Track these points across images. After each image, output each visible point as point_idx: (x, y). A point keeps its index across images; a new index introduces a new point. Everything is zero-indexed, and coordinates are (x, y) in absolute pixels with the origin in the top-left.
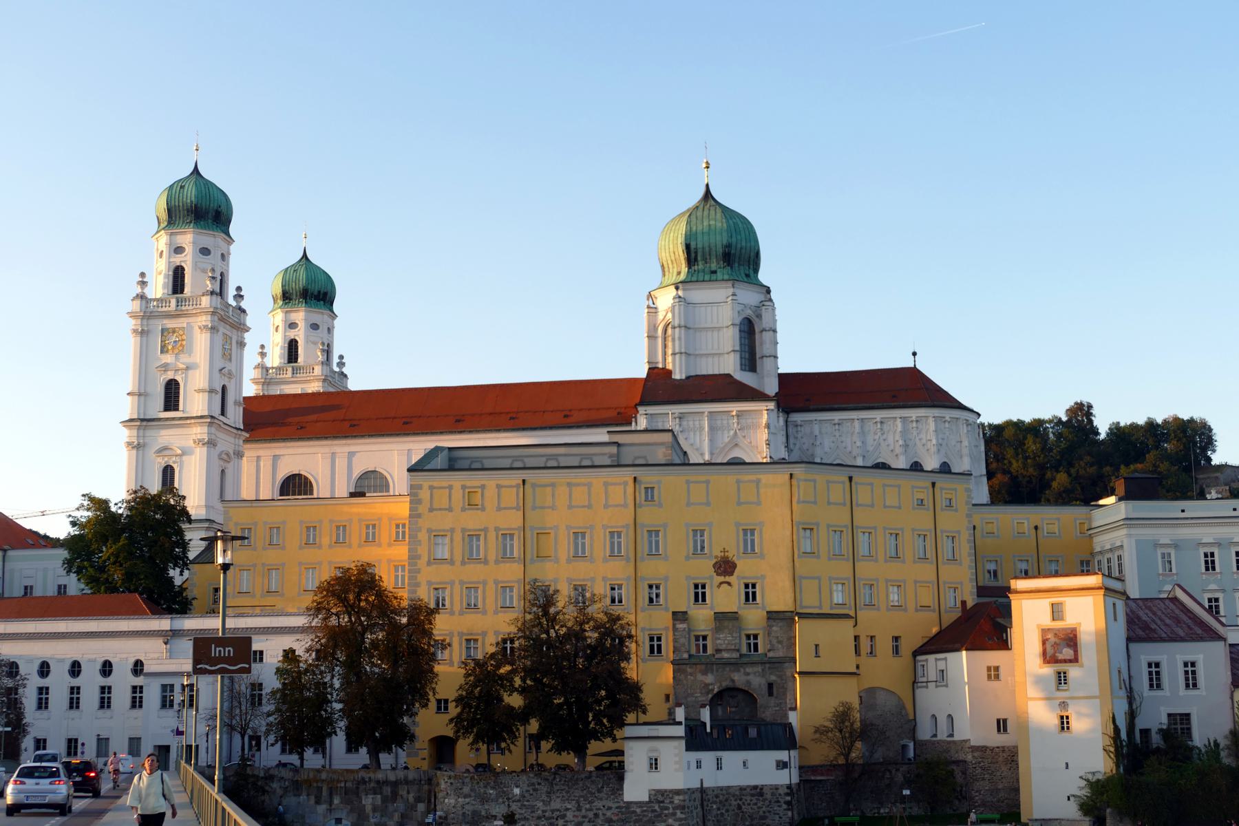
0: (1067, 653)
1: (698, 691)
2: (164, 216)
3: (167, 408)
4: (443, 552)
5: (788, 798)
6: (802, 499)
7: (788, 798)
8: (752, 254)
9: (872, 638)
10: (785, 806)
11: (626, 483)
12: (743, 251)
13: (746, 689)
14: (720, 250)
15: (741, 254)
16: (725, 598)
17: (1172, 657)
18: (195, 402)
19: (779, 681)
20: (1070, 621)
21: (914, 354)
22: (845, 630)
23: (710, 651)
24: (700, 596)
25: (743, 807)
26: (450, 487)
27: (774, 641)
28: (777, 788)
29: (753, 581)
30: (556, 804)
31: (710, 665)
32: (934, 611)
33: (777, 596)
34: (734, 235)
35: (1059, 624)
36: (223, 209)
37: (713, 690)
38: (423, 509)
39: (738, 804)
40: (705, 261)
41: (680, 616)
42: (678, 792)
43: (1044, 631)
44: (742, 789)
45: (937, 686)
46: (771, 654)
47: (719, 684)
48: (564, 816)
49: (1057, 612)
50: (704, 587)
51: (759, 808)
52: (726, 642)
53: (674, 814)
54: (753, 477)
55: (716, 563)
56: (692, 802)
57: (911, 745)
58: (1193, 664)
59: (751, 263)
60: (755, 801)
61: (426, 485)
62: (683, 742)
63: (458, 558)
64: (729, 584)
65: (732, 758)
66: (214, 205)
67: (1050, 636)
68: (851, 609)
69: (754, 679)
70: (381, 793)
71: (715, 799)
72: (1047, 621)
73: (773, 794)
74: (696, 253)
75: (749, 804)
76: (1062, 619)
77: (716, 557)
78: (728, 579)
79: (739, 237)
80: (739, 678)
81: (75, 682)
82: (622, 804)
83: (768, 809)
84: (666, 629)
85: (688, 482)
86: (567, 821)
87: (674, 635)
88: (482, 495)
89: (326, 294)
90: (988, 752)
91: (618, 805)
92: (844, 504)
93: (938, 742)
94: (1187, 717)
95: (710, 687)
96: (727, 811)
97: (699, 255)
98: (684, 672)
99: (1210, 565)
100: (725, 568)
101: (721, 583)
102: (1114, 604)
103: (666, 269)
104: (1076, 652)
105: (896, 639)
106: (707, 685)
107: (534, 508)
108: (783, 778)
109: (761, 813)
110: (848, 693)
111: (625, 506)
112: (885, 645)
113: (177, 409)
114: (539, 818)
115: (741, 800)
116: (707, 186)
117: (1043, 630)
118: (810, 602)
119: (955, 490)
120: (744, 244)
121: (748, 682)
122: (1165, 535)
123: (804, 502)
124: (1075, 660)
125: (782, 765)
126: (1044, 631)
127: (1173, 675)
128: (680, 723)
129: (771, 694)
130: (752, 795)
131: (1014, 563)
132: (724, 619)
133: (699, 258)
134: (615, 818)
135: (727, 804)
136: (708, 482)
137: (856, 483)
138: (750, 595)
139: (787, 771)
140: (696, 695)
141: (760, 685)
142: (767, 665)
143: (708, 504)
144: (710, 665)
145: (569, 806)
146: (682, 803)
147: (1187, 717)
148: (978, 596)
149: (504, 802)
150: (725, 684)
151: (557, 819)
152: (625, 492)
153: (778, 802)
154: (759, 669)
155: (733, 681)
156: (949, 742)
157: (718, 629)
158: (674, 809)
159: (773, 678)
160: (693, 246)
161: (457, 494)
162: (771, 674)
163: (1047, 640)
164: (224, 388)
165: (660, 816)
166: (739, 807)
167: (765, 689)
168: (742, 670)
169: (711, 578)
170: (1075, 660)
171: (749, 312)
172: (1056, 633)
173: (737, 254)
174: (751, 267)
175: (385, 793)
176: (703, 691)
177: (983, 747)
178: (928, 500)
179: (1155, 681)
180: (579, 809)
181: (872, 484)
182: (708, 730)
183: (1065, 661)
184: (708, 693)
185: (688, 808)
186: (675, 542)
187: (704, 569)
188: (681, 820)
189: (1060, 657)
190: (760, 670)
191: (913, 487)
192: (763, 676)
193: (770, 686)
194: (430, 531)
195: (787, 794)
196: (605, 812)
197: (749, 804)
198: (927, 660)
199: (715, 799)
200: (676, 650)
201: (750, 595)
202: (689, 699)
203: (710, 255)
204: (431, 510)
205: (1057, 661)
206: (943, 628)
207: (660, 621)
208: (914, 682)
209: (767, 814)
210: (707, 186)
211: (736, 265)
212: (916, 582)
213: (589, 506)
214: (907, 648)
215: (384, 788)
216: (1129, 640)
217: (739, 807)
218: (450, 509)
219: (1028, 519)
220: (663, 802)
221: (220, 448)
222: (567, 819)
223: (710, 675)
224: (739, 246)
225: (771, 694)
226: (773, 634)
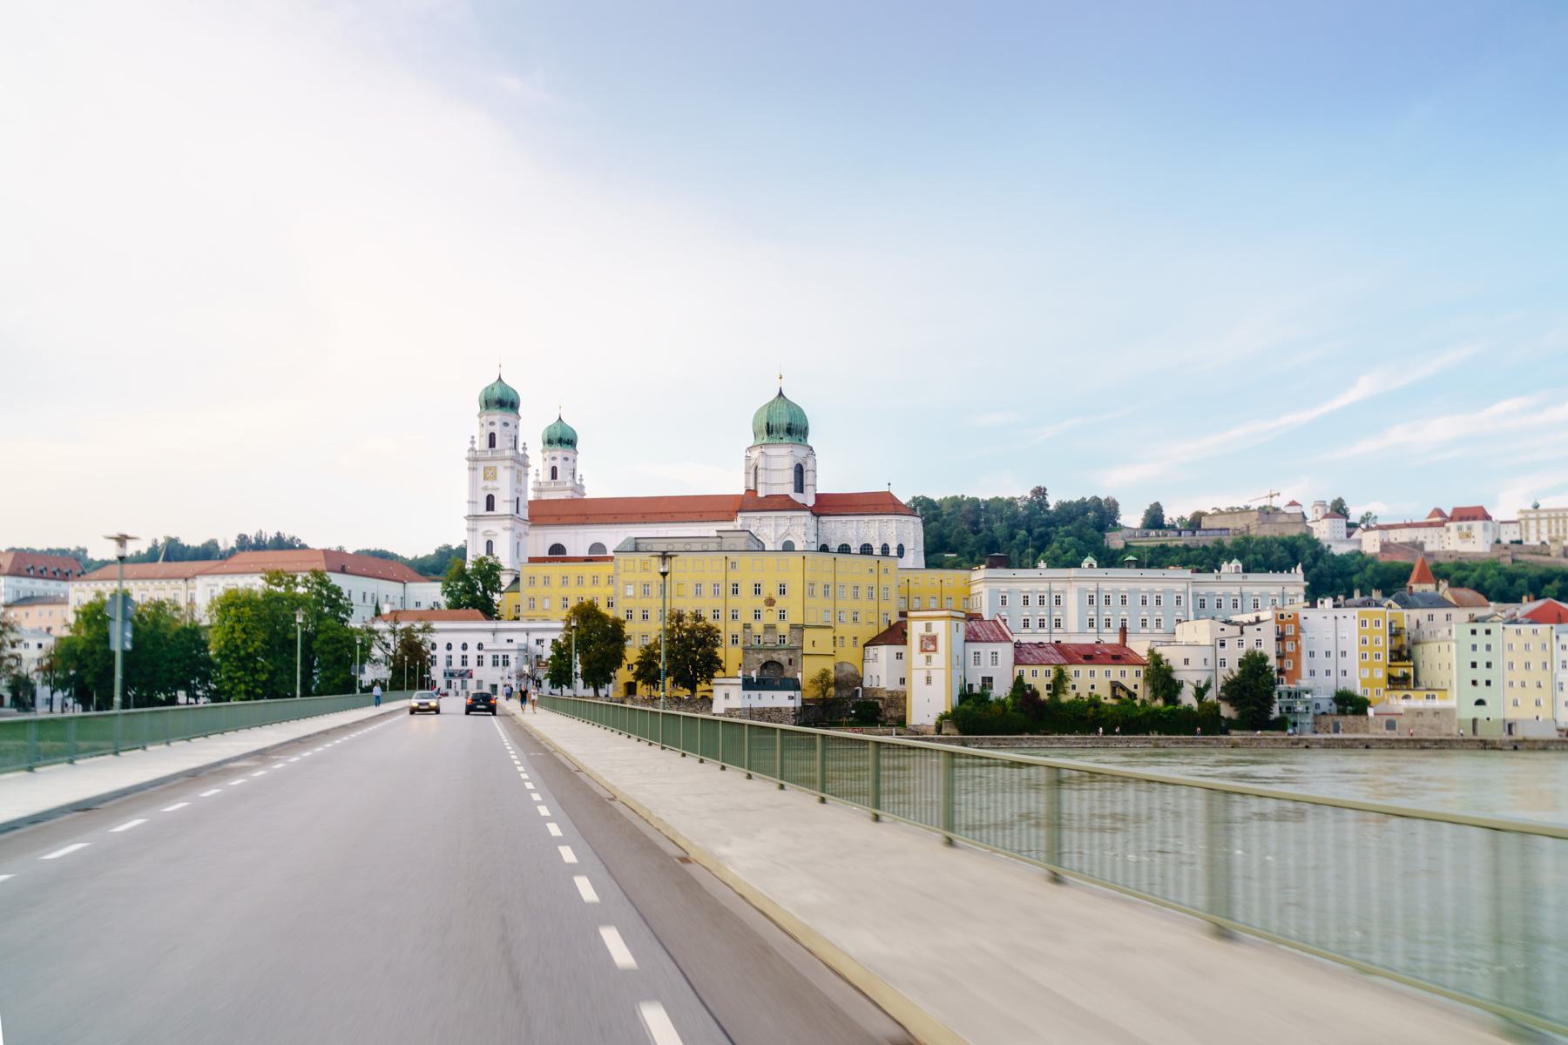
0: (932, 647)
2: (484, 404)
3: (488, 510)
4: (630, 592)
9: (843, 638)
11: (721, 560)
14: (785, 427)
16: (770, 617)
17: (986, 649)
18: (502, 507)
20: (934, 631)
21: (889, 484)
22: (829, 633)
23: (761, 643)
24: (757, 616)
26: (634, 561)
28: (788, 708)
33: (795, 617)
35: (929, 634)
36: (515, 401)
38: (621, 571)
40: (778, 432)
41: (747, 626)
42: (738, 709)
43: (922, 637)
44: (771, 709)
49: (928, 627)
50: (759, 611)
54: (785, 558)
57: (861, 689)
61: (622, 559)
62: (741, 687)
63: (638, 595)
65: (766, 694)
66: (510, 399)
69: (782, 657)
72: (923, 632)
78: (771, 608)
80: (775, 657)
81: (449, 653)
89: (572, 441)
93: (873, 688)
94: (990, 679)
98: (748, 653)
99: (1026, 602)
102: (957, 625)
105: (856, 638)
108: (791, 704)
110: (829, 665)
112: (849, 641)
113: (493, 510)
116: (781, 389)
118: (811, 621)
121: (780, 659)
122: (1004, 587)
124: (935, 651)
125: (791, 698)
126: (922, 637)
129: (790, 664)
132: (770, 628)
138: (782, 617)
139: (793, 701)
147: (990, 679)
150: (768, 659)
154: (785, 652)
157: (765, 632)
159: (792, 657)
160: (770, 424)
161: (638, 563)
164: (518, 499)
167: (787, 661)
170: (935, 651)
171: (800, 461)
186: (746, 589)
187: (759, 602)
189: (929, 649)
193: (790, 660)
194: (624, 582)
200: (744, 642)
201: (782, 617)
204: (625, 571)
205: (927, 651)
206: (880, 632)
208: (864, 660)
210: (781, 389)
214: (861, 643)
216: (966, 641)
218: (634, 571)
221: (517, 531)
225: (790, 664)
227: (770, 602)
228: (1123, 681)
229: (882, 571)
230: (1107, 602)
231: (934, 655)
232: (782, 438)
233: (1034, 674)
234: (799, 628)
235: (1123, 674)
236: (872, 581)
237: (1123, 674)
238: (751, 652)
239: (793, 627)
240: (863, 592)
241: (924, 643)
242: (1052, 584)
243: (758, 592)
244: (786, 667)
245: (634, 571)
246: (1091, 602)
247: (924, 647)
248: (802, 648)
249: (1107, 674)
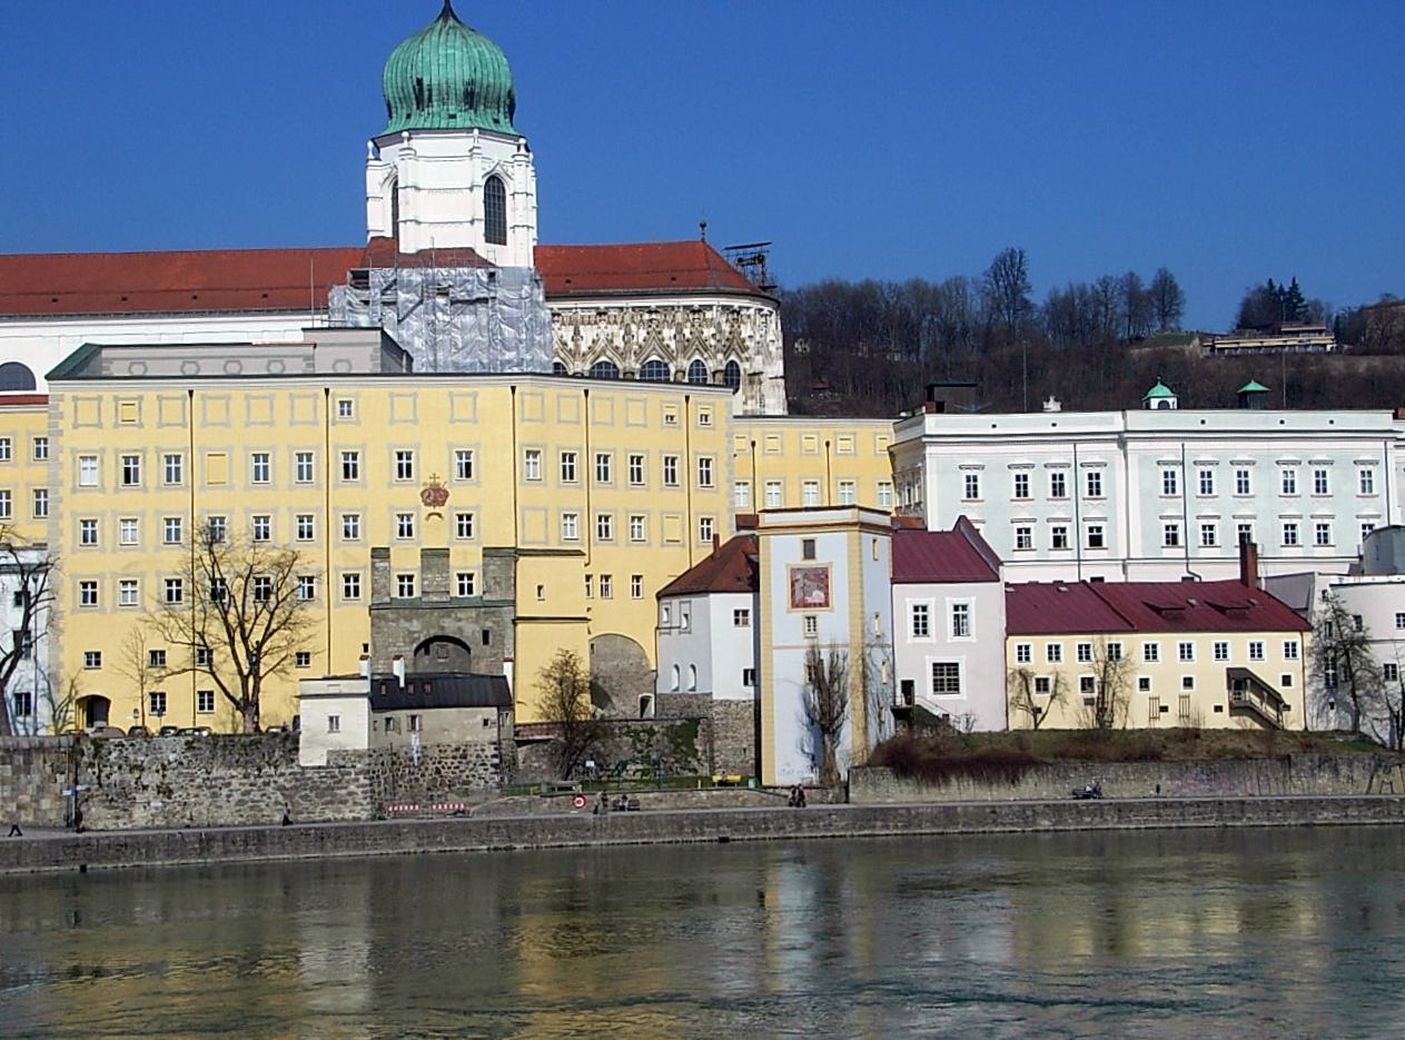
0: (818, 596)
4: (89, 478)
5: (496, 761)
6: (526, 416)
7: (496, 761)
8: (503, 94)
9: (607, 578)
10: (492, 770)
12: (491, 90)
13: (457, 636)
14: (460, 88)
15: (488, 93)
19: (495, 627)
20: (820, 560)
23: (417, 593)
24: (406, 531)
25: (443, 771)
26: (100, 399)
27: (492, 582)
29: (468, 512)
31: (414, 609)
32: (683, 546)
34: (479, 69)
35: (810, 563)
37: (419, 638)
38: (63, 425)
39: (437, 768)
40: (443, 102)
41: (380, 554)
43: (794, 571)
45: (680, 633)
46: (487, 597)
47: (425, 632)
48: (229, 784)
49: (809, 549)
51: (461, 771)
53: (357, 780)
55: (425, 491)
56: (379, 767)
57: (653, 696)
58: (924, 609)
59: (502, 104)
60: (456, 764)
63: (110, 484)
64: (439, 515)
67: (799, 576)
68: (583, 544)
69: (469, 629)
70: (11, 763)
71: (408, 763)
72: (797, 558)
73: (478, 756)
74: (430, 90)
75: (449, 768)
76: (813, 557)
77: (424, 484)
78: (438, 510)
79: (485, 72)
80: (450, 626)
82: (296, 770)
83: (473, 773)
84: (365, 567)
85: (391, 395)
86: (231, 790)
87: (373, 575)
88: (140, 409)
90: (733, 706)
91: (291, 770)
92: (578, 423)
95: (416, 635)
96: (423, 775)
97: (435, 92)
98: (384, 618)
100: (435, 497)
101: (432, 514)
103: (393, 110)
104: (827, 594)
105: (638, 578)
107: (204, 424)
109: (464, 777)
110: (577, 642)
111: (315, 423)
112: (621, 585)
114: (199, 787)
115: (440, 763)
117: (827, 569)
118: (531, 538)
119: (713, 404)
120: (491, 80)
121: (460, 630)
123: (530, 420)
126: (794, 571)
127: (942, 621)
128: (365, 678)
129: (486, 641)
130: (454, 758)
131: (801, 486)
132: (435, 557)
133: (434, 98)
134: (288, 786)
135: (422, 768)
136: (415, 395)
137: (593, 397)
138: (465, 527)
142: (483, 610)
143: (415, 421)
144: (414, 609)
145: (234, 773)
146: (366, 768)
148: (739, 528)
149: (157, 771)
150: (433, 632)
151: (220, 789)
152: (315, 409)
153: (484, 764)
154: (473, 613)
155: (442, 628)
156: (691, 696)
157: (425, 568)
158: (356, 774)
159: (489, 624)
160: (426, 82)
162: (487, 619)
163: (797, 581)
165: (340, 781)
166: (438, 771)
167: (480, 637)
168: (453, 615)
169: (418, 508)
172: (807, 573)
173: (483, 95)
174: (502, 109)
175: (16, 763)
176: (407, 640)
177: (727, 701)
178: (680, 418)
179: (921, 627)
181: (612, 399)
182: (402, 684)
183: (815, 605)
184: (412, 643)
185: (374, 772)
187: (409, 496)
188: (363, 786)
189: (809, 600)
190: (474, 615)
191: (662, 401)
192: (477, 622)
193: (486, 634)
194: (73, 451)
195: (494, 756)
196: (276, 778)
197: (449, 768)
198: (670, 603)
199: (408, 763)
201: (465, 530)
202: (390, 649)
203: (448, 94)
206: (694, 565)
207: (357, 557)
209: (471, 779)
211: (482, 107)
212: (662, 513)
213: (271, 423)
215: (16, 757)
217: (438, 771)
218: (99, 425)
219: (818, 433)
220: (344, 767)
222: (232, 787)
223: (415, 622)
224: (485, 82)
225: (486, 641)
226: (490, 574)
227: (435, 496)
228: (1257, 668)
229: (695, 419)
230: (1206, 487)
231: (819, 613)
232: (453, 117)
233: (1054, 653)
234: (504, 557)
235: (1256, 651)
236: (672, 442)
237: (1256, 651)
238: (391, 615)
239: (488, 553)
240: (653, 470)
241: (797, 586)
242: (1078, 446)
243: (405, 471)
244: (477, 647)
245: (99, 425)
246: (1170, 486)
247: (799, 595)
248: (513, 603)
249: (1221, 652)
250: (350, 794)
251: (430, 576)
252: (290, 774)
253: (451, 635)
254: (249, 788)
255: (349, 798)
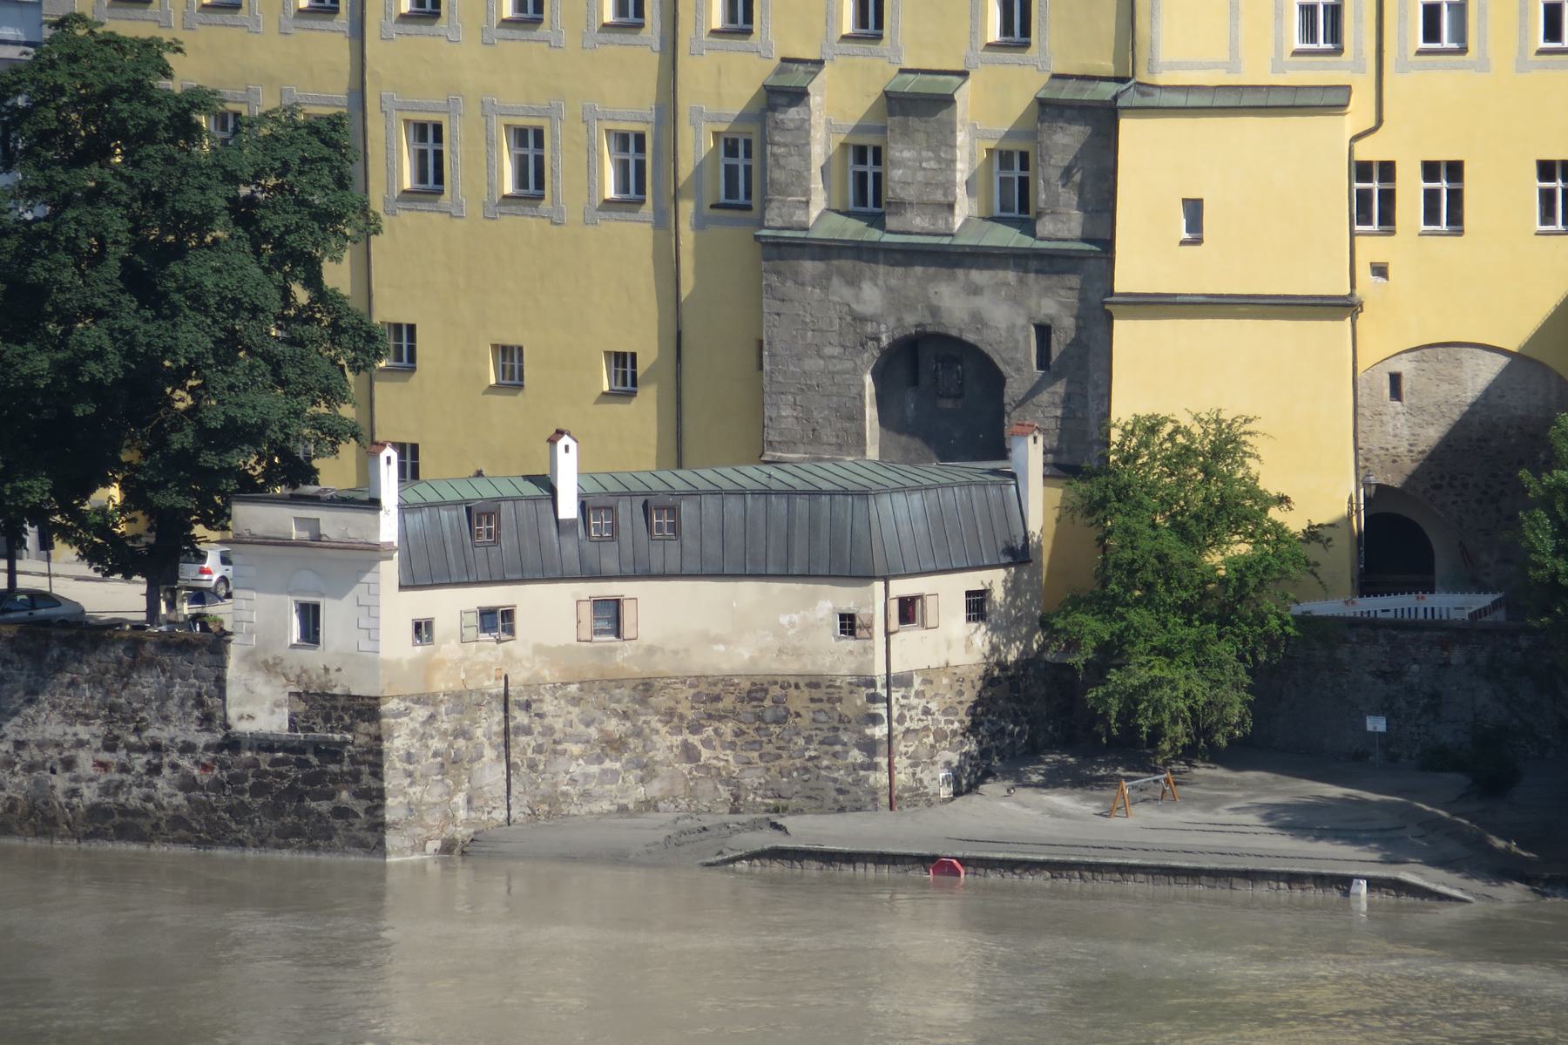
1: (835, 339)
30: (53, 728)
48: (69, 764)
52: (920, 176)
53: (356, 777)
95: (870, 328)
106: (860, 319)
121: (978, 319)
134: (204, 778)
140: (828, 351)
141: (1011, 328)
145: (84, 736)
150: (911, 320)
155: (934, 311)
180: (110, 745)
182: (568, 508)
192: (1015, 300)
250: (342, 813)
251: (906, 154)
252: (207, 748)
253: (954, 333)
254: (117, 777)
255: (338, 823)
